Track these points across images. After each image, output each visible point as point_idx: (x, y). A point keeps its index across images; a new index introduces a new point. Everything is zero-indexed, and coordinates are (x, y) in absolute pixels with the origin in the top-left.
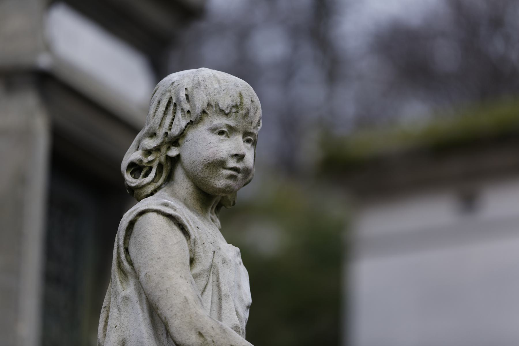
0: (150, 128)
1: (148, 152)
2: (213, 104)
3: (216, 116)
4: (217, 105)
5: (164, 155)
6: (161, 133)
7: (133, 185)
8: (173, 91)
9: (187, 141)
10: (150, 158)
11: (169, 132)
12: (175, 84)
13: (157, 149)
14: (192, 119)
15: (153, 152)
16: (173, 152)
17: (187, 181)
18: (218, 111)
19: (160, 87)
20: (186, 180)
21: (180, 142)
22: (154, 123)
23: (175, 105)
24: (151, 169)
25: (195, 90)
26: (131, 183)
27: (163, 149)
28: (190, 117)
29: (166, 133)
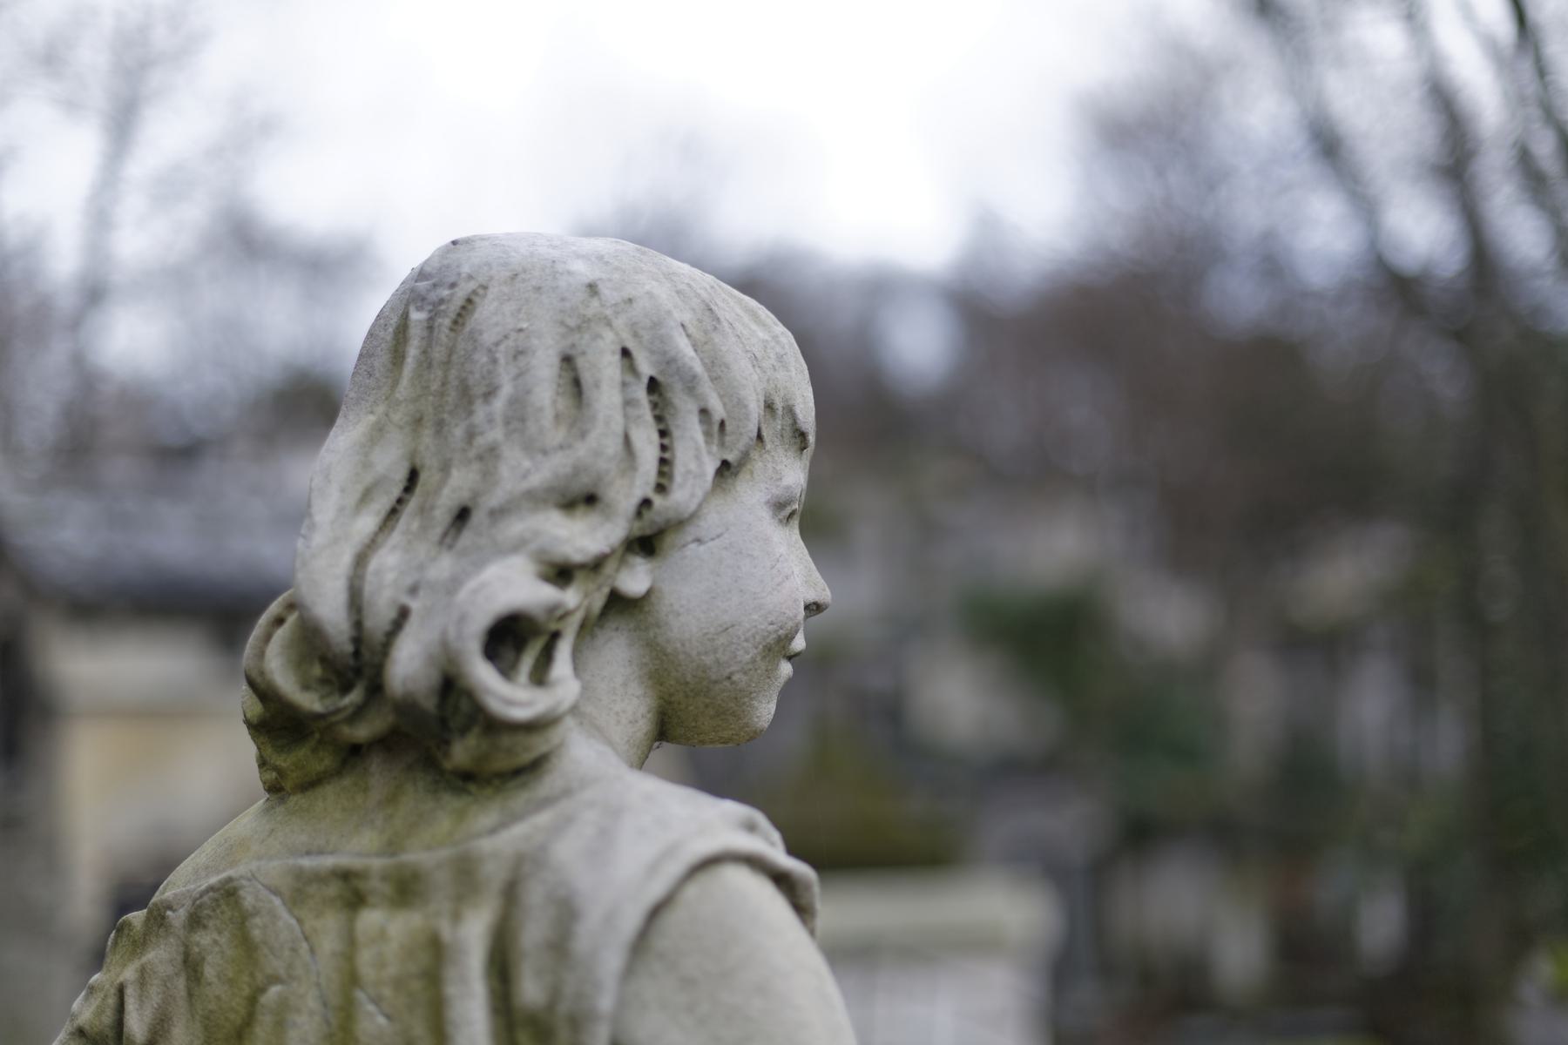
0: (577, 470)
1: (562, 574)
2: (779, 405)
3: (781, 451)
4: (790, 410)
5: (606, 590)
6: (625, 495)
7: (520, 714)
8: (619, 322)
9: (699, 541)
10: (571, 597)
11: (658, 501)
12: (605, 290)
13: (596, 565)
14: (730, 457)
15: (580, 576)
16: (635, 579)
17: (639, 692)
18: (788, 433)
19: (493, 291)
20: (636, 689)
21: (669, 539)
22: (597, 453)
23: (653, 385)
24: (555, 636)
25: (717, 338)
26: (510, 703)
27: (609, 568)
28: (722, 444)
29: (646, 503)
